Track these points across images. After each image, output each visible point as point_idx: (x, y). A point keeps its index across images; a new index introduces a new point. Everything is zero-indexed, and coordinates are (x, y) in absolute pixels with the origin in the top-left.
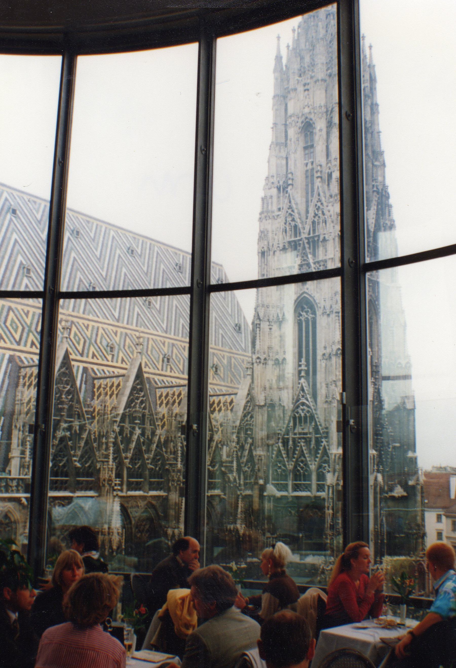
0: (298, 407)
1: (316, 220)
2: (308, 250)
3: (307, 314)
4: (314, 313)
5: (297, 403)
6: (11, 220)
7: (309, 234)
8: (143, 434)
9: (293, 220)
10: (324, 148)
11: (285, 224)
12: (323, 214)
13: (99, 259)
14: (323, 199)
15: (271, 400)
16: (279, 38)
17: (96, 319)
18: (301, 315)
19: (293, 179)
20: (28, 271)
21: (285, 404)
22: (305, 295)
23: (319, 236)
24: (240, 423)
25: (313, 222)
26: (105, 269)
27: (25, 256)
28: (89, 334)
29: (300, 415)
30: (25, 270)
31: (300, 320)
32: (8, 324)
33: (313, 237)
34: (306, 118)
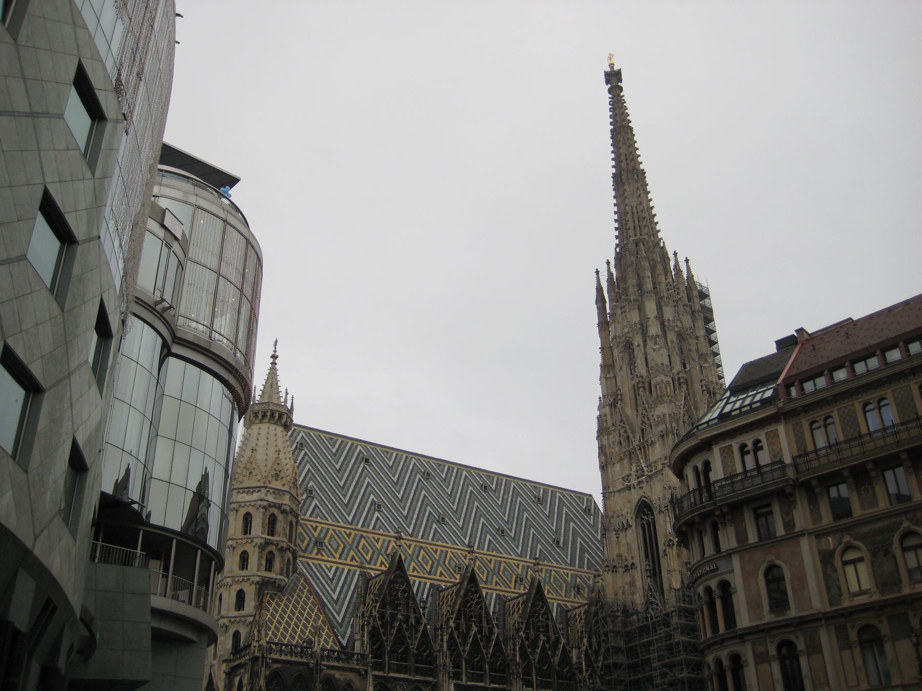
1: (643, 427)
2: (640, 456)
3: (648, 517)
4: (653, 515)
6: (364, 468)
8: (480, 631)
9: (625, 432)
10: (643, 359)
13: (450, 496)
16: (597, 272)
17: (445, 544)
18: (643, 519)
19: (621, 395)
20: (379, 506)
25: (642, 430)
26: (456, 504)
27: (376, 495)
28: (437, 557)
29: (651, 615)
30: (377, 505)
32: (360, 548)
34: (626, 337)
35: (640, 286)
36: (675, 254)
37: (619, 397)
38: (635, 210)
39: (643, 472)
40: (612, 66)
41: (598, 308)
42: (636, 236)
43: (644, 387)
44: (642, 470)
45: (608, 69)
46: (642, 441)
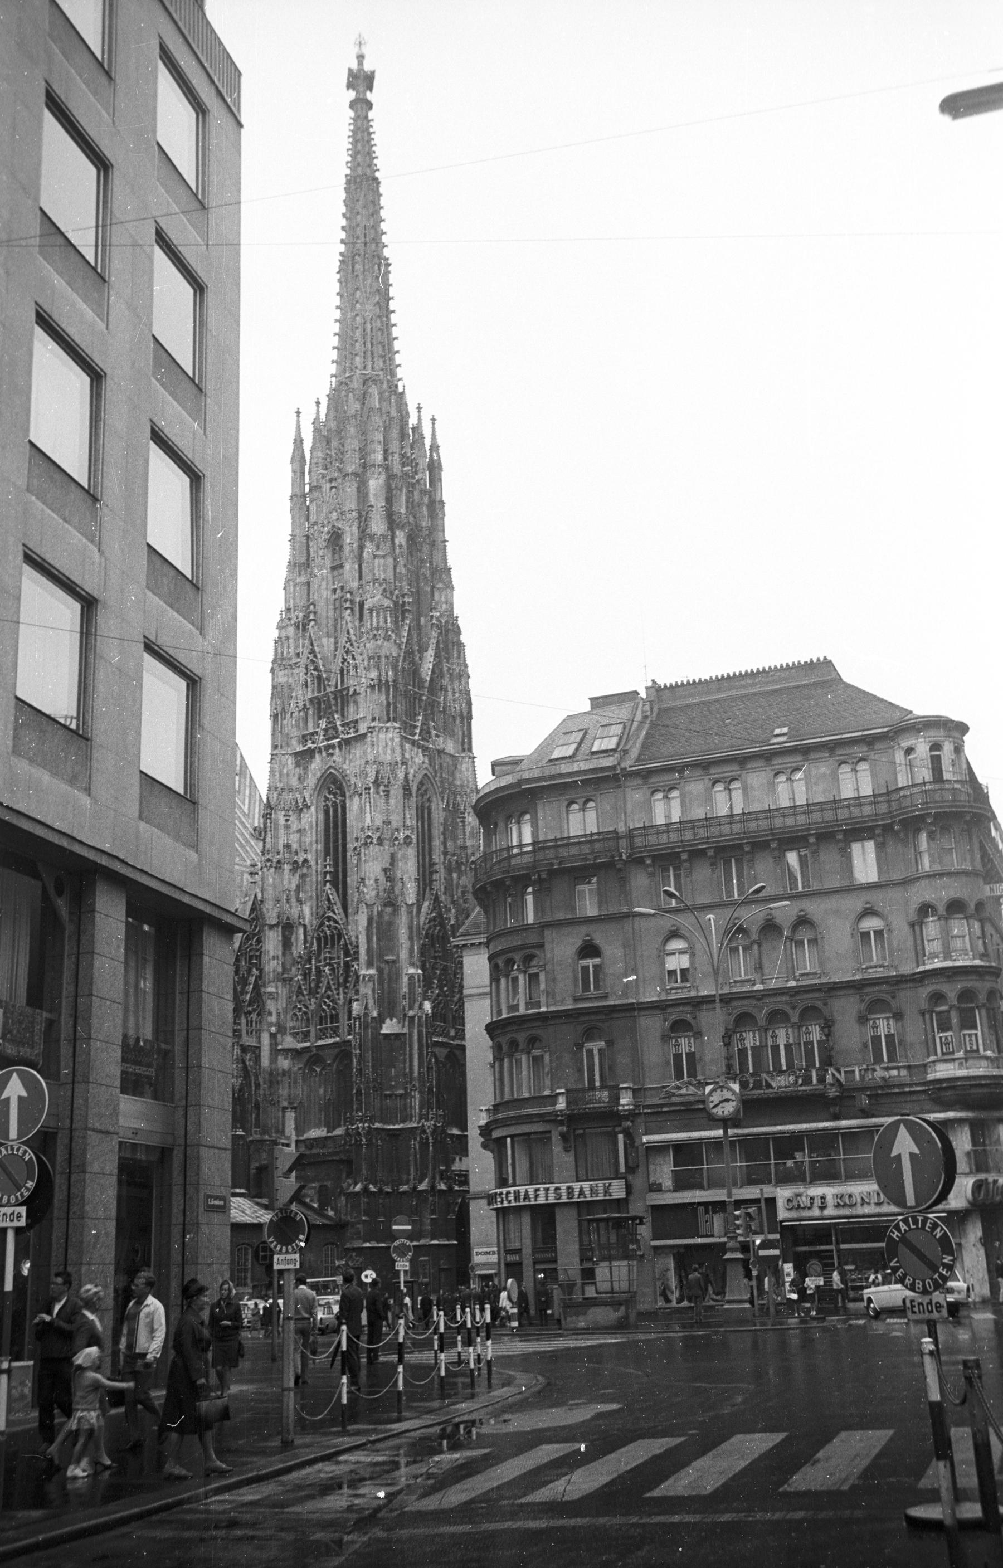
0: (322, 924)
4: (343, 795)
5: (322, 918)
7: (336, 687)
9: (316, 669)
11: (306, 674)
12: (354, 658)
14: (353, 638)
15: (288, 918)
16: (298, 413)
19: (315, 613)
21: (307, 922)
22: (332, 771)
23: (348, 689)
24: (240, 947)
31: (327, 805)
33: (341, 691)
34: (334, 526)
35: (363, 453)
36: (419, 408)
37: (312, 617)
38: (369, 326)
39: (337, 732)
40: (361, 58)
41: (294, 471)
42: (365, 368)
43: (352, 609)
44: (335, 728)
45: (354, 66)
46: (339, 687)
